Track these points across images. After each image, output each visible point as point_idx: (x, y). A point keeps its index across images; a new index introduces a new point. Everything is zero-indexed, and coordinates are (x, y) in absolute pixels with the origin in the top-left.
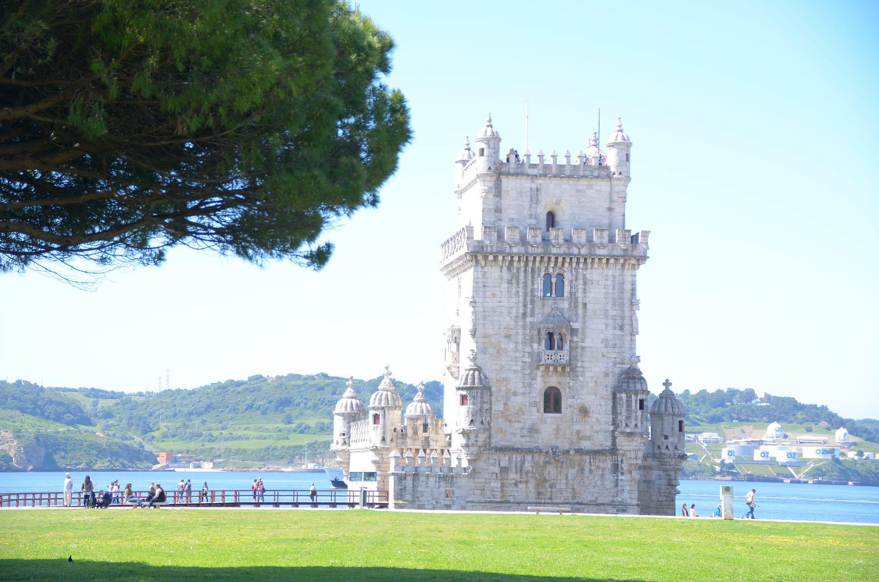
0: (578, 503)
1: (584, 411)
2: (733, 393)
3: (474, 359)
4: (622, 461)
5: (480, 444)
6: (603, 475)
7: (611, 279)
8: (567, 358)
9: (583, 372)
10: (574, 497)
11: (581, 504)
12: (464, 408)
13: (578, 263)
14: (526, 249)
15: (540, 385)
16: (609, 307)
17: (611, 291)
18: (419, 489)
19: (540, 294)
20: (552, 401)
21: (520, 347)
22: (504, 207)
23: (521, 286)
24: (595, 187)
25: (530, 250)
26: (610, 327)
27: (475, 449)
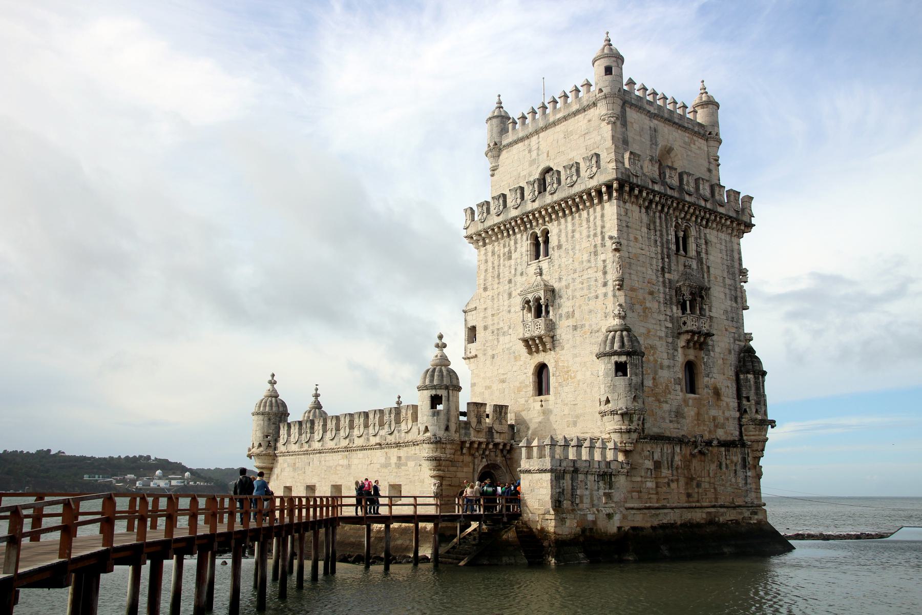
1: (717, 393)
2: (141, 457)
3: (623, 318)
8: (707, 326)
9: (713, 346)
11: (721, 506)
12: (621, 381)
13: (702, 220)
14: (665, 189)
16: (725, 275)
17: (725, 257)
18: (579, 492)
19: (674, 247)
21: (662, 309)
22: (630, 140)
23: (658, 233)
25: (669, 192)
27: (634, 436)
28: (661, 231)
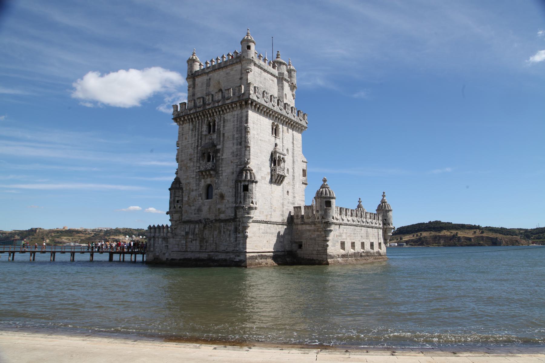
0: (216, 252)
1: (222, 196)
4: (239, 225)
5: (174, 219)
6: (230, 234)
7: (236, 116)
9: (222, 173)
10: (216, 249)
13: (219, 112)
15: (203, 183)
16: (235, 133)
17: (236, 123)
20: (209, 191)
21: (195, 164)
24: (234, 69)
25: (198, 110)
26: (235, 145)
28: (198, 129)
